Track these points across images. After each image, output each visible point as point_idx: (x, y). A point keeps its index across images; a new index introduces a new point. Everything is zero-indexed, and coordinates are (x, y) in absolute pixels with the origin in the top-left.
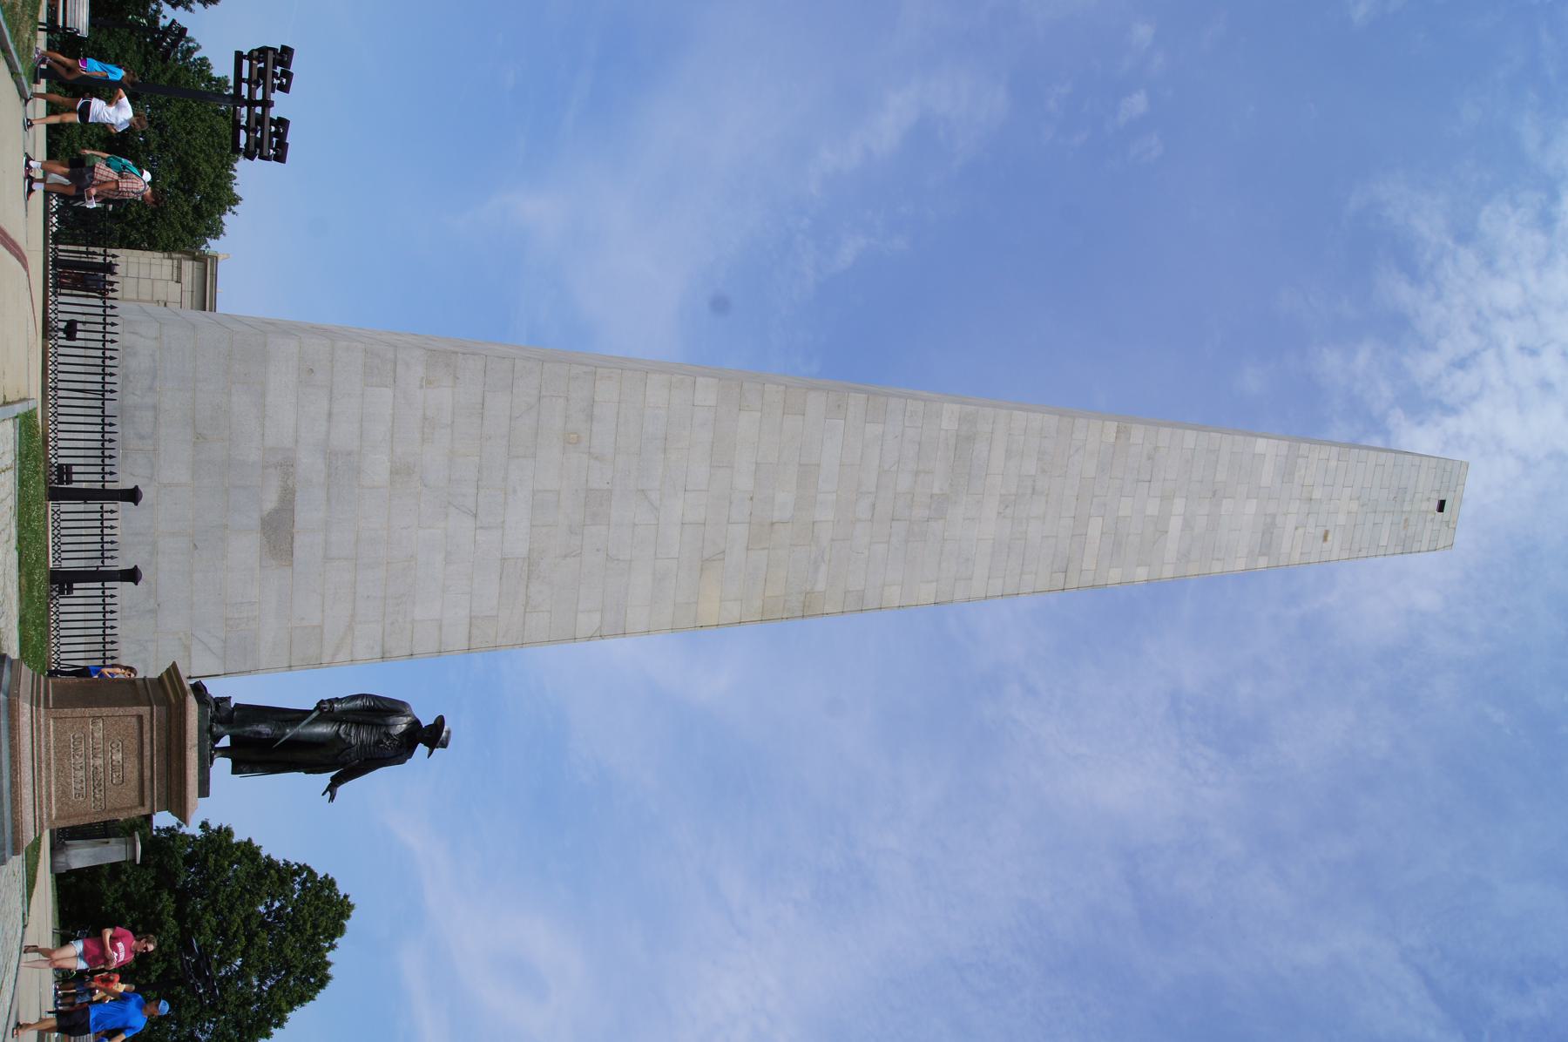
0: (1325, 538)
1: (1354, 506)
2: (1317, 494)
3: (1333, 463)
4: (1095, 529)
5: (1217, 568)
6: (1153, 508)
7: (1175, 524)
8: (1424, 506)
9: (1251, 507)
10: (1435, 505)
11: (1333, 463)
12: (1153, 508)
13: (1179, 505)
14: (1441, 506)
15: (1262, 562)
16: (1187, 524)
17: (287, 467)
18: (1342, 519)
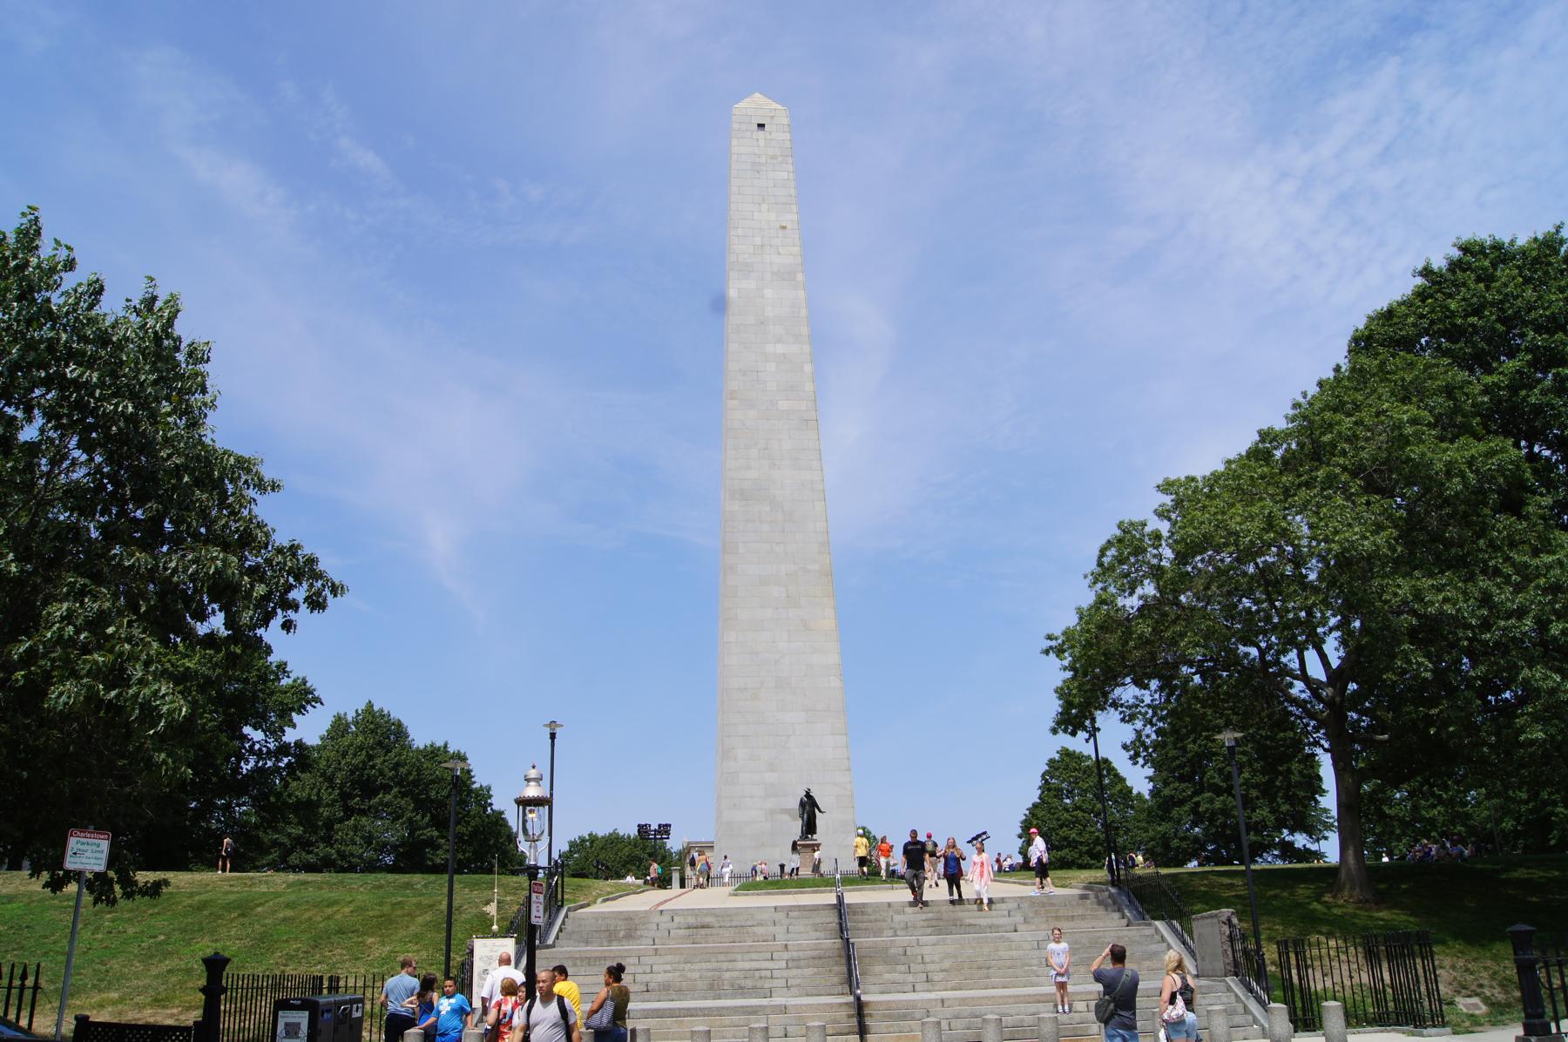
0: (784, 228)
1: (765, 207)
2: (758, 241)
3: (740, 232)
4: (783, 405)
5: (804, 312)
6: (771, 367)
7: (780, 349)
8: (762, 143)
9: (769, 293)
10: (761, 133)
11: (740, 232)
12: (771, 367)
13: (770, 348)
14: (761, 126)
15: (800, 277)
16: (779, 341)
17: (772, 812)
18: (773, 216)
